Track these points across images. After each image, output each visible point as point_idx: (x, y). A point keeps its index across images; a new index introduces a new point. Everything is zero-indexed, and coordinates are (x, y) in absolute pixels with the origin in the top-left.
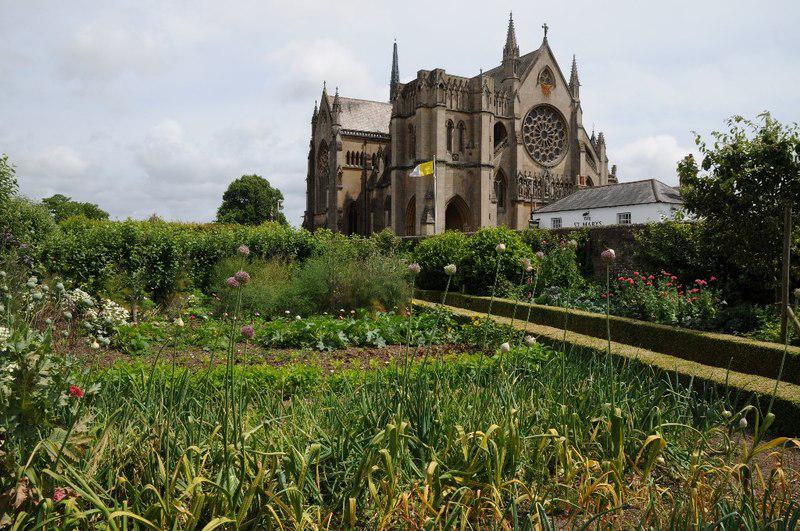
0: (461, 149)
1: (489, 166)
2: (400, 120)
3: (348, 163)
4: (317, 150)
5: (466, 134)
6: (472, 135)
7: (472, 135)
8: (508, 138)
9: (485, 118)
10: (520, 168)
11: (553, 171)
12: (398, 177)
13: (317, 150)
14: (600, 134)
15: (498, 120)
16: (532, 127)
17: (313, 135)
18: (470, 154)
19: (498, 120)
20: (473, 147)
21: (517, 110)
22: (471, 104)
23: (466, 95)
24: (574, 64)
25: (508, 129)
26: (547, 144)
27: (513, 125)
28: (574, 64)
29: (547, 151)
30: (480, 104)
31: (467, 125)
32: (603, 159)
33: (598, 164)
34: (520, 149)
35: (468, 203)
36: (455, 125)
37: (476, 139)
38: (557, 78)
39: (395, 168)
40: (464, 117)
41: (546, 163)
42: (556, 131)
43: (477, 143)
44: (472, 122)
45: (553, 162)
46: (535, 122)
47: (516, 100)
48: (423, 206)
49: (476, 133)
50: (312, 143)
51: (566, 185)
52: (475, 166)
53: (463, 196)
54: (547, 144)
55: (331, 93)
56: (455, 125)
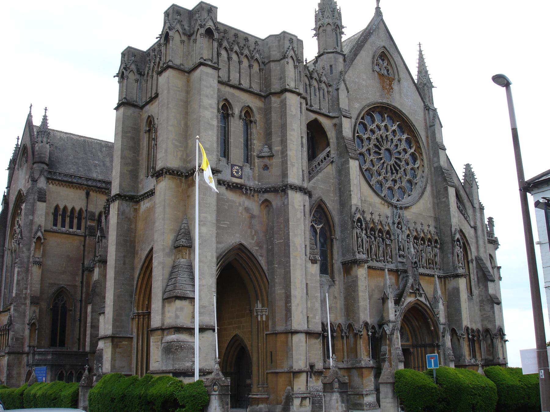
0: (248, 159)
1: (301, 189)
2: (131, 111)
3: (55, 224)
4: (11, 206)
5: (257, 131)
6: (268, 135)
7: (268, 135)
8: (332, 149)
9: (292, 101)
10: (355, 201)
11: (407, 214)
12: (120, 214)
13: (11, 206)
14: (468, 167)
15: (313, 116)
16: (369, 139)
17: (9, 187)
18: (266, 167)
19: (313, 116)
20: (271, 157)
21: (344, 104)
22: (266, 81)
23: (256, 67)
24: (420, 51)
25: (331, 134)
26: (395, 168)
27: (338, 127)
28: (420, 51)
29: (395, 181)
30: (282, 78)
31: (257, 117)
32: (477, 206)
33: (470, 212)
34: (354, 165)
35: (263, 261)
36: (237, 111)
37: (276, 139)
38: (403, 74)
39: (119, 196)
40: (254, 103)
41: (394, 201)
42: (405, 150)
43: (277, 148)
44: (267, 112)
45: (406, 200)
46: (373, 132)
47: (342, 86)
48: (169, 261)
49: (275, 129)
50: (6, 199)
51: (429, 240)
52: (274, 190)
53: (254, 249)
54: (395, 168)
55: (37, 122)
56: (237, 111)
